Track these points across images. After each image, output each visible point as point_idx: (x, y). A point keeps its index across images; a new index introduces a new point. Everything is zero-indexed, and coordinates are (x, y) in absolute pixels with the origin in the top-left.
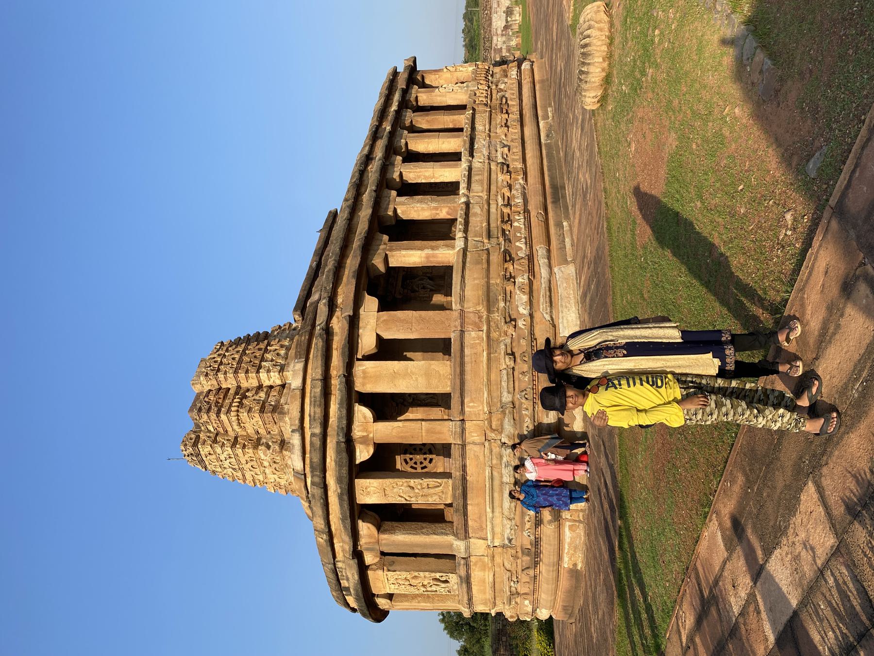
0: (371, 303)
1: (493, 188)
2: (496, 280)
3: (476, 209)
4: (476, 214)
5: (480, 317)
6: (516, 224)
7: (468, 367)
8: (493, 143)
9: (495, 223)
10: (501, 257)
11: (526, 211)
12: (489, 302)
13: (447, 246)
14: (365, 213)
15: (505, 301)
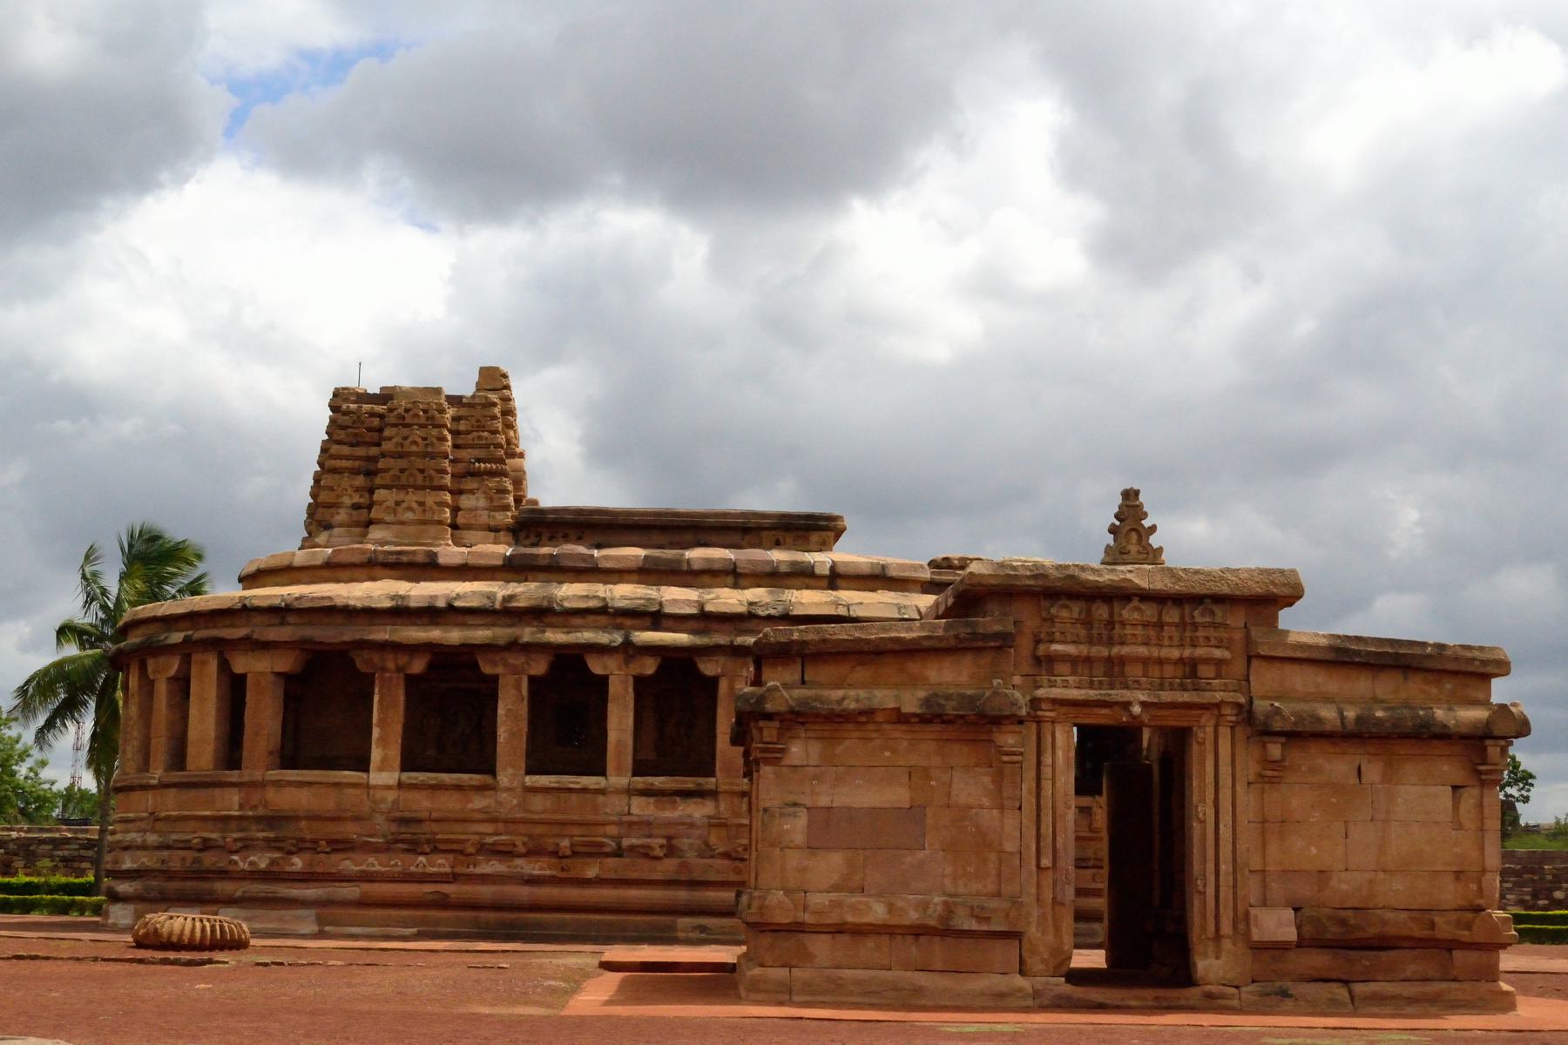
0: (285, 663)
1: (539, 830)
2: (305, 829)
3: (479, 802)
4: (470, 801)
5: (254, 807)
6: (422, 859)
7: (202, 792)
8: (697, 832)
9: (442, 833)
10: (339, 837)
11: (454, 878)
12: (272, 820)
13: (384, 760)
14: (453, 636)
15: (266, 840)
